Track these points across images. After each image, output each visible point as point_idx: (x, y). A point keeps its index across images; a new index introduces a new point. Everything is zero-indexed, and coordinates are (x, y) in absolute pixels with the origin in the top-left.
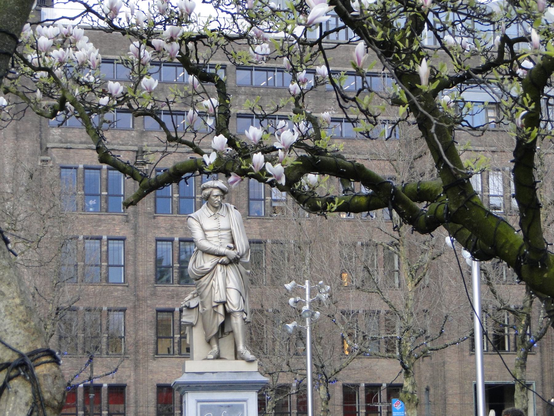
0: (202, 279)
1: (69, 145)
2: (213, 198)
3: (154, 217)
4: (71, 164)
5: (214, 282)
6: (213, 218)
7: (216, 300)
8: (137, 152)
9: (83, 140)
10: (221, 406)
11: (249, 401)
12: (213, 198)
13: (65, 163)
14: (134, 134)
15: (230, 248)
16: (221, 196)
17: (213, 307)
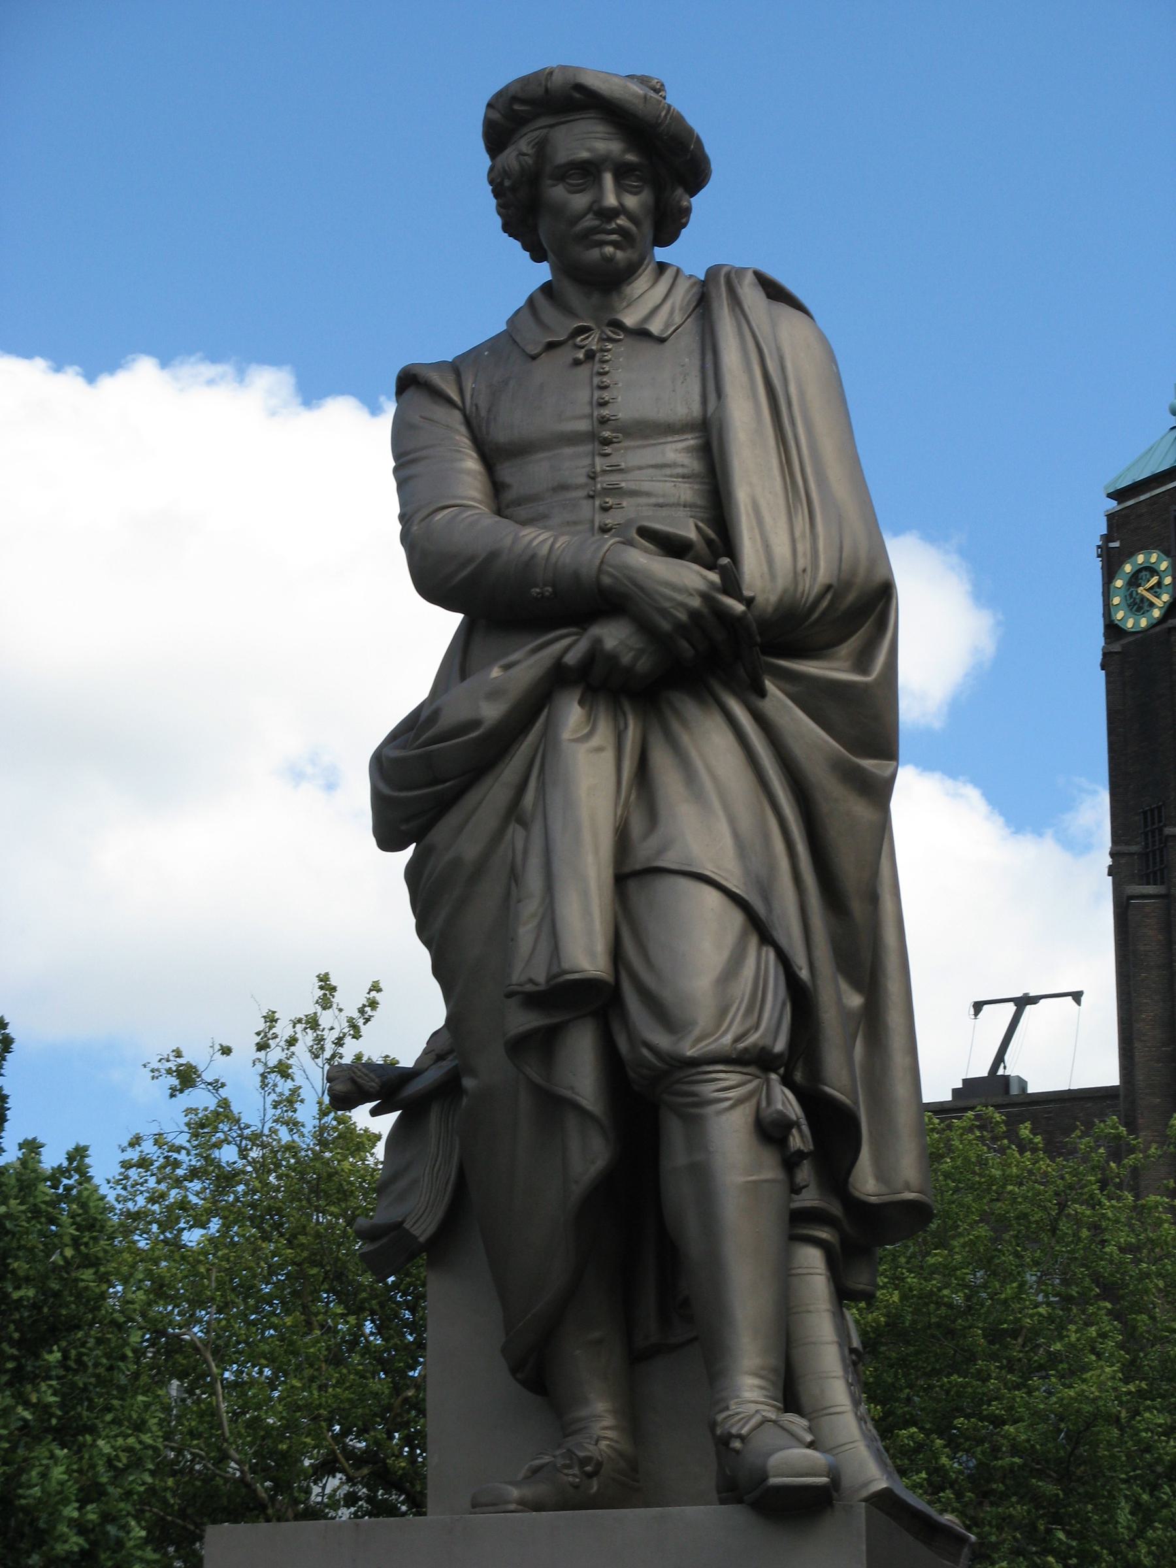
0: (439, 834)
2: (558, 192)
5: (520, 833)
6: (565, 355)
7: (518, 975)
12: (558, 192)
15: (673, 547)
16: (622, 172)
17: (518, 1046)
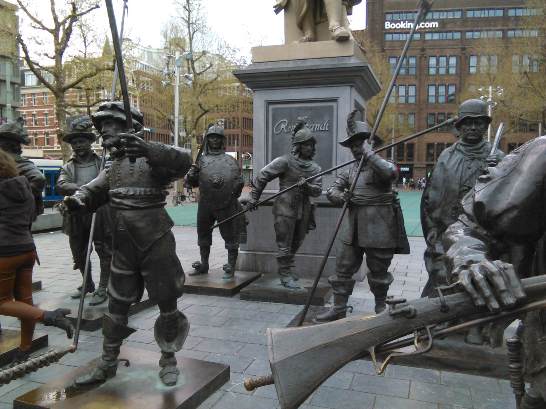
1: (393, 48)
3: (428, 76)
4: (394, 55)
8: (422, 49)
9: (399, 46)
10: (300, 108)
11: (340, 101)
13: (391, 55)
14: (420, 42)
